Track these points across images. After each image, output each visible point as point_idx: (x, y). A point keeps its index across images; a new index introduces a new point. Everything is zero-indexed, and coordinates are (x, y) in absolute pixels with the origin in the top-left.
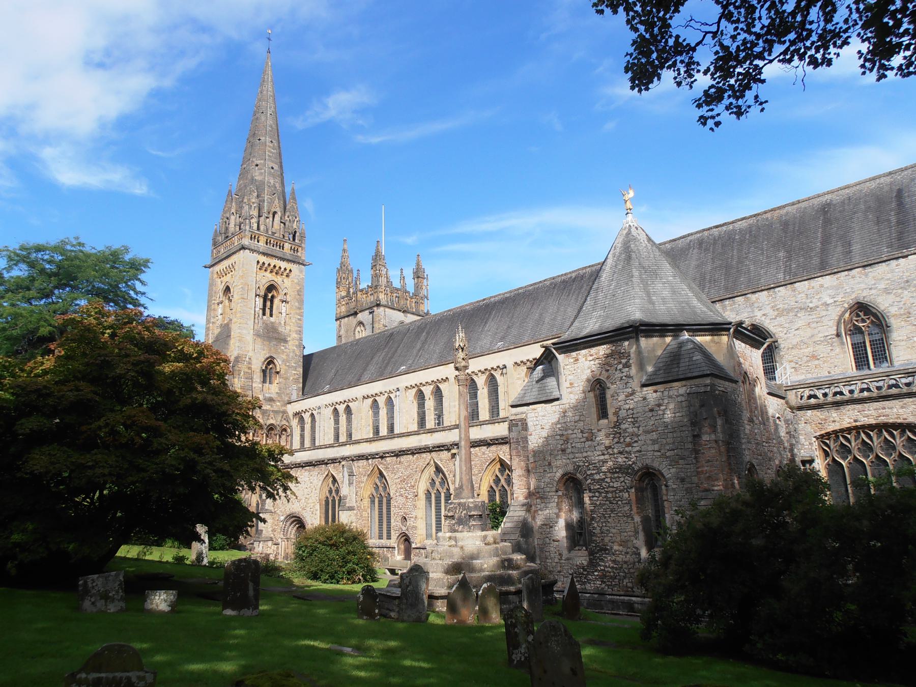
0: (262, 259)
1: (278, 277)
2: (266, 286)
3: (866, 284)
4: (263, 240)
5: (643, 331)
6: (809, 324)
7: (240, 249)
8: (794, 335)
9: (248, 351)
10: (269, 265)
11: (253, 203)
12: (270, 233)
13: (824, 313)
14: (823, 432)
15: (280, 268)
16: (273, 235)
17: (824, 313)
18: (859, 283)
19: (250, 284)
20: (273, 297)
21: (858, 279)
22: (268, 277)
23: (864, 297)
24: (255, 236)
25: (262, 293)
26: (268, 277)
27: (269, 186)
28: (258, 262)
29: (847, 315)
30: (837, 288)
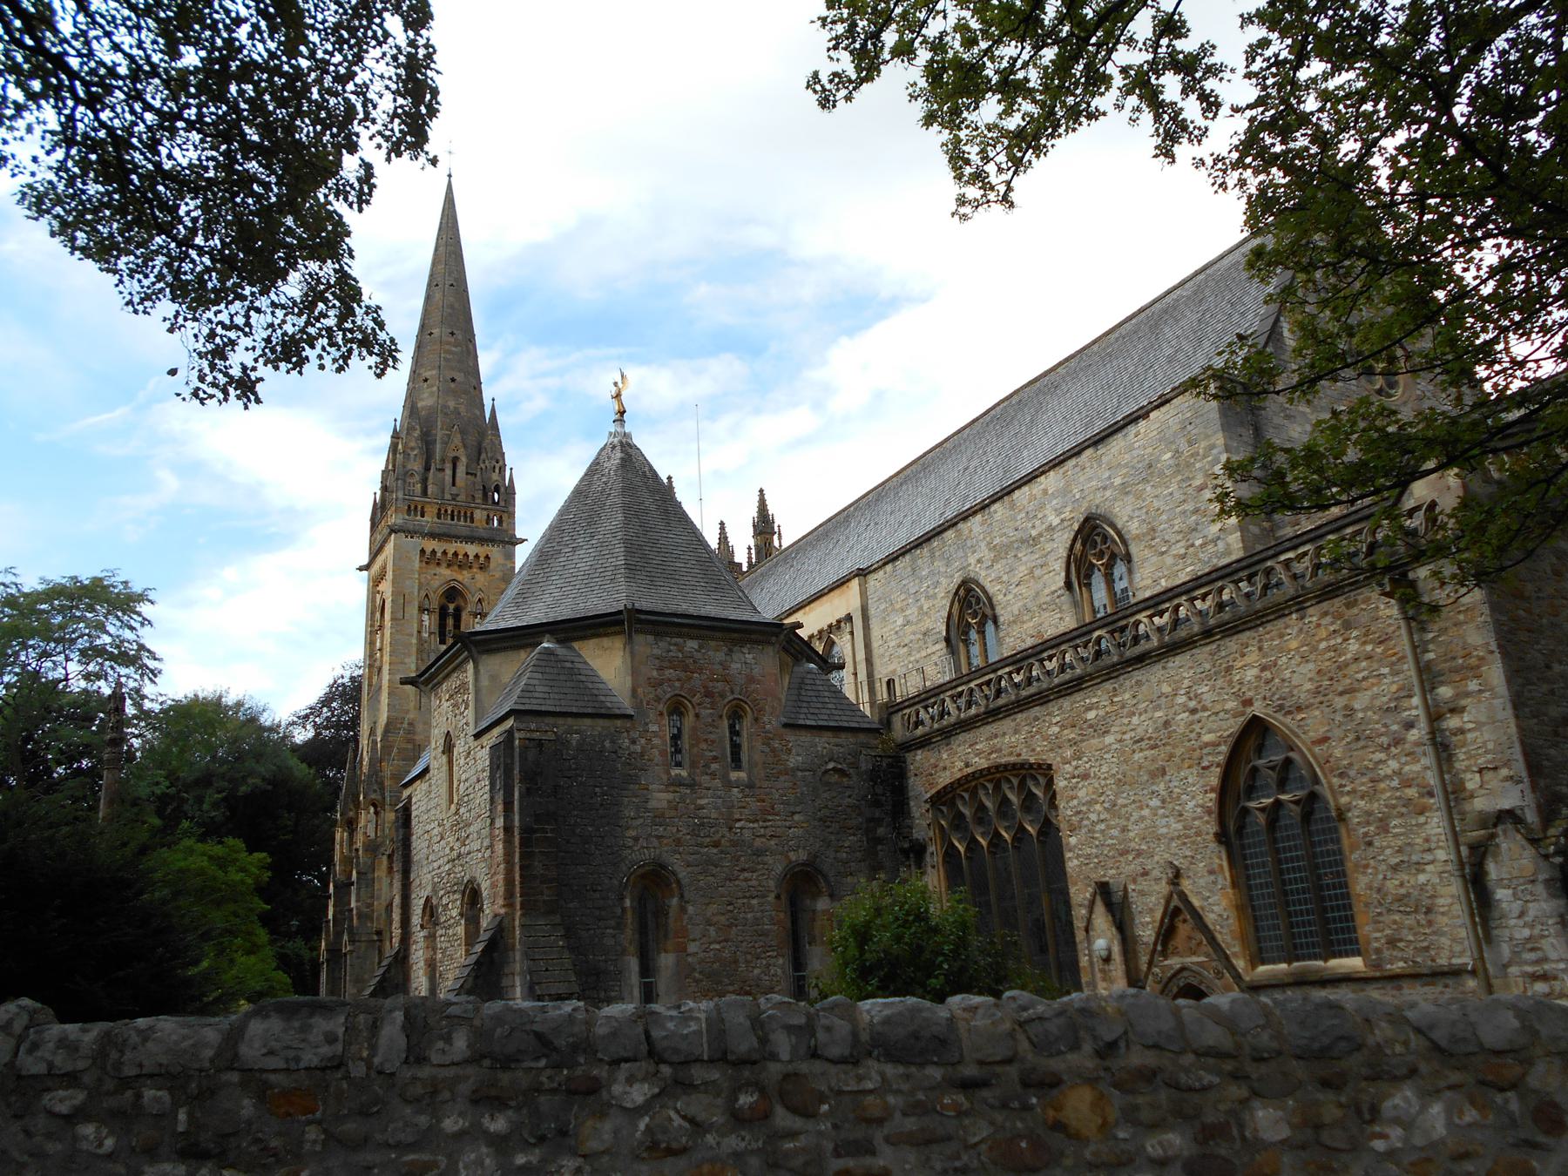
0: (431, 545)
1: (465, 572)
2: (441, 591)
3: (1100, 480)
4: (431, 511)
5: (477, 644)
6: (1032, 572)
7: (390, 534)
8: (1015, 595)
9: (407, 712)
10: (445, 553)
11: (412, 449)
12: (447, 496)
13: (1048, 547)
14: (933, 791)
15: (466, 555)
16: (454, 499)
17: (1048, 547)
18: (1090, 479)
19: (407, 592)
20: (458, 611)
21: (1089, 472)
22: (445, 575)
23: (1097, 507)
24: (416, 507)
25: (435, 605)
26: (445, 575)
27: (446, 414)
28: (423, 551)
29: (1078, 546)
30: (1065, 492)
